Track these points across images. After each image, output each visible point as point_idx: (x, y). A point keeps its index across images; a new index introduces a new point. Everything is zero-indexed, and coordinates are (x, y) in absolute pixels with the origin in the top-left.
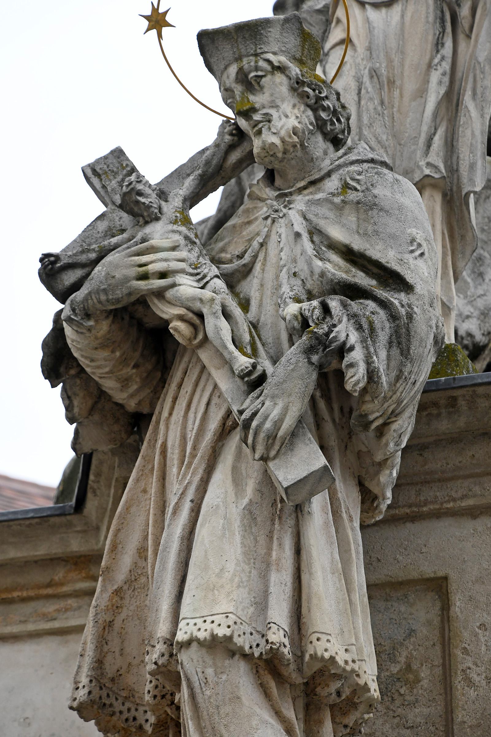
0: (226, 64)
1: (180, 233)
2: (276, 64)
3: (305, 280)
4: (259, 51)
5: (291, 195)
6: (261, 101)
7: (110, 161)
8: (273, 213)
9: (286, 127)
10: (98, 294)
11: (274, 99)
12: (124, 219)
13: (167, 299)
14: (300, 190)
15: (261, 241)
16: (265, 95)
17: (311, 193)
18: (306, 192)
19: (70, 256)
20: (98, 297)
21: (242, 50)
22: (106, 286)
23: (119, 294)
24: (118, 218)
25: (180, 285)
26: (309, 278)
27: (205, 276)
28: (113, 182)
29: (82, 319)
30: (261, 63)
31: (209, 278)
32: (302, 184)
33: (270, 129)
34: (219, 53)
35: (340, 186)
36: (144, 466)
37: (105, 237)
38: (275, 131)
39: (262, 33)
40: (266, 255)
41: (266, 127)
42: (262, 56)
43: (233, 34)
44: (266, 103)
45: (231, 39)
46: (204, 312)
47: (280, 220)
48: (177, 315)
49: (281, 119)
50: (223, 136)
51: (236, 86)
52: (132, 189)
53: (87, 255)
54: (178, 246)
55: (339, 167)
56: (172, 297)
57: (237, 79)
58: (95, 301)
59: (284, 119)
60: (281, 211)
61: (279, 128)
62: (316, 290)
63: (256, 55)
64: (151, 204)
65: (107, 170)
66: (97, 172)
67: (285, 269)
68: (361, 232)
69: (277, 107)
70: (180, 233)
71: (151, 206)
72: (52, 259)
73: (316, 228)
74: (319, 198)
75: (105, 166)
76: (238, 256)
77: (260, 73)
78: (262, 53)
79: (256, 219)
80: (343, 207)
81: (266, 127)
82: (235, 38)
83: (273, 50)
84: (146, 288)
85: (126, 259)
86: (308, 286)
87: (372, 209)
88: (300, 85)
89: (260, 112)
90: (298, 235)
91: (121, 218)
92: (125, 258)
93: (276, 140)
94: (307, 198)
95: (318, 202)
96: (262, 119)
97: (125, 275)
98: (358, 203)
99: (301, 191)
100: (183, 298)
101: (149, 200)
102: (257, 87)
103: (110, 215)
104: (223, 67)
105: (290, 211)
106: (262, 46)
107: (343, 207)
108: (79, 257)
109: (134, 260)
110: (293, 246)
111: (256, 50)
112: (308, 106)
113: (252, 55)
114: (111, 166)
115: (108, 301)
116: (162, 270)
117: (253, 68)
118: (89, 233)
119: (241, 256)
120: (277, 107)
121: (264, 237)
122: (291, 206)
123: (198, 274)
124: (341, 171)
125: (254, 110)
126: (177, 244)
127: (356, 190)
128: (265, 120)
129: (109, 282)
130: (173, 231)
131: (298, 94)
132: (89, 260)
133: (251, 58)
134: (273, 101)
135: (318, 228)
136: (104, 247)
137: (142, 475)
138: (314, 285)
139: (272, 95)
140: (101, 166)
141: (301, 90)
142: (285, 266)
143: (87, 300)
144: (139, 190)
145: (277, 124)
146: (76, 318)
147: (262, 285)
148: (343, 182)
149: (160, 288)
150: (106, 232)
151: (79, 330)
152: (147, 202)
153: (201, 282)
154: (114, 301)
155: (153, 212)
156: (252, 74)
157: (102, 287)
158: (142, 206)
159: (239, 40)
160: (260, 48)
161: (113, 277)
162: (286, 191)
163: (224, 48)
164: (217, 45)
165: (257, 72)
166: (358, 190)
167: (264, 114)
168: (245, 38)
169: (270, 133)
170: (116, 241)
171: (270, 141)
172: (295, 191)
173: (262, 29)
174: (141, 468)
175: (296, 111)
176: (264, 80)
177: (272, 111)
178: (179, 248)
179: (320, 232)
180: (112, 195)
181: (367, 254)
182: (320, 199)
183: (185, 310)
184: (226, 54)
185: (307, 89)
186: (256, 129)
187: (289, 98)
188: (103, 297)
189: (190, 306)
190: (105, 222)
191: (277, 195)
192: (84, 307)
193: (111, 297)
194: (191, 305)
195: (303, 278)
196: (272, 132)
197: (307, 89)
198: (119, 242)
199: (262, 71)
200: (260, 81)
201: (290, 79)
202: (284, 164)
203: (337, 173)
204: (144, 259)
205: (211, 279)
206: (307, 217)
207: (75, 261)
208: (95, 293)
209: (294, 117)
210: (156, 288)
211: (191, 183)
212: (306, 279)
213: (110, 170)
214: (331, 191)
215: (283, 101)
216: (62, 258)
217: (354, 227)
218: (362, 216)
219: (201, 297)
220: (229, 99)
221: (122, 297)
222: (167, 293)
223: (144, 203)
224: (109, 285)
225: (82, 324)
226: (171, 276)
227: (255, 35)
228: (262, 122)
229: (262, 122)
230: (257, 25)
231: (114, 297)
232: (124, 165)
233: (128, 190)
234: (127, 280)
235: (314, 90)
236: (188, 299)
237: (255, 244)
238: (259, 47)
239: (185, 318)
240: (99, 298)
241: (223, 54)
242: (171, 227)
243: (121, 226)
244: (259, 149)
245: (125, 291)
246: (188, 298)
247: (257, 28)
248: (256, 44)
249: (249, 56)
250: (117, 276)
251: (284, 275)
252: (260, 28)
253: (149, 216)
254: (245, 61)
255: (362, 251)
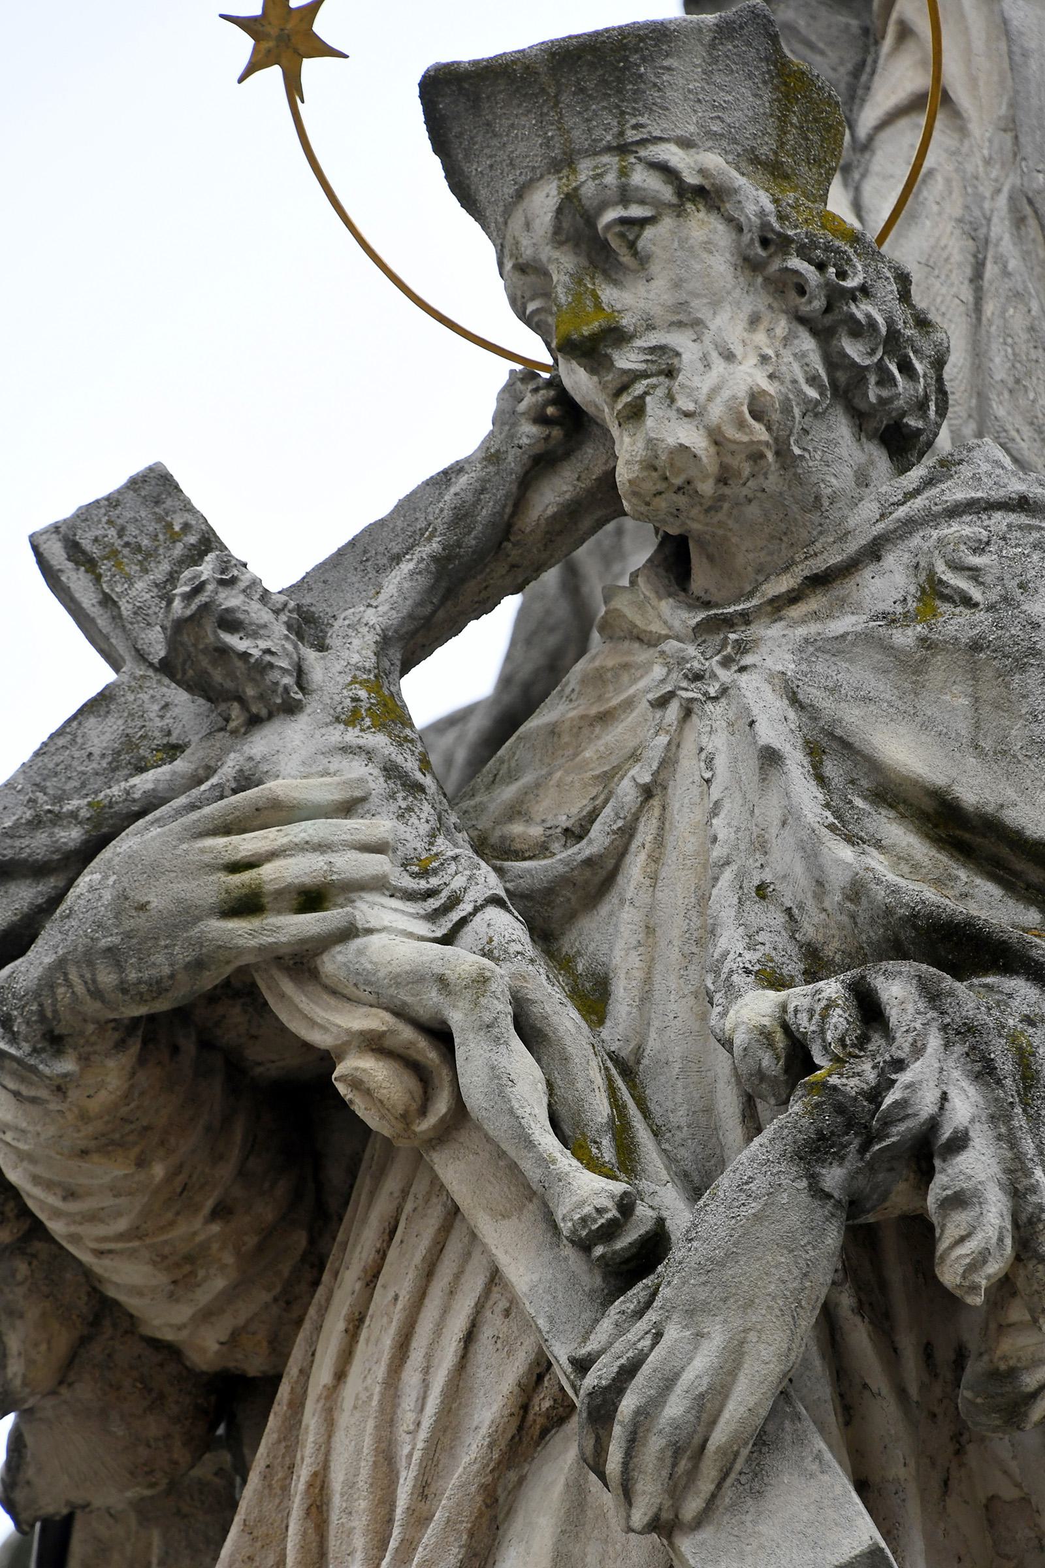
1: (368, 754)
2: (692, 179)
3: (795, 911)
4: (632, 136)
6: (642, 304)
9: (726, 394)
10: (91, 964)
11: (684, 297)
12: (176, 711)
13: (327, 981)
14: (778, 606)
15: (647, 778)
16: (654, 284)
17: (815, 616)
18: (796, 611)
20: (88, 976)
21: (576, 133)
22: (116, 940)
23: (160, 964)
24: (156, 707)
25: (369, 931)
26: (810, 903)
27: (454, 901)
29: (35, 1051)
30: (641, 178)
32: (783, 584)
33: (671, 398)
34: (495, 142)
35: (912, 589)
37: (114, 770)
38: (691, 407)
39: (641, 76)
40: (661, 828)
41: (660, 392)
42: (643, 153)
43: (544, 79)
44: (657, 311)
45: (536, 96)
46: (451, 1023)
47: (709, 707)
48: (362, 1033)
49: (708, 366)
50: (514, 425)
51: (556, 254)
52: (205, 607)
53: (51, 835)
54: (363, 799)
55: (910, 525)
56: (342, 974)
57: (557, 230)
58: (80, 989)
59: (719, 366)
60: (714, 676)
61: (702, 398)
62: (835, 944)
63: (623, 149)
64: (268, 658)
65: (118, 543)
66: (84, 552)
67: (728, 875)
68: (987, 744)
69: (696, 325)
70: (368, 754)
71: (271, 666)
73: (831, 735)
74: (841, 631)
75: (112, 532)
76: (567, 831)
77: (636, 211)
78: (643, 142)
79: (629, 704)
80: (924, 660)
81: (660, 392)
82: (552, 91)
83: (679, 132)
84: (253, 943)
85: (185, 846)
86: (809, 930)
87: (1023, 668)
88: (772, 249)
89: (638, 343)
90: (770, 758)
91: (166, 706)
92: (181, 840)
93: (691, 437)
94: (802, 631)
95: (838, 647)
96: (642, 366)
97: (180, 901)
98: (976, 646)
99: (779, 609)
100: (381, 974)
101: (263, 644)
102: (626, 258)
103: (131, 697)
104: (509, 190)
105: (744, 678)
107: (924, 660)
108: (26, 842)
109: (211, 850)
110: (753, 797)
111: (622, 134)
112: (802, 320)
113: (609, 149)
114: (132, 530)
115: (123, 988)
116: (307, 880)
117: (613, 193)
118: (57, 759)
119: (577, 830)
120: (696, 325)
121: (655, 767)
122: (748, 660)
124: (916, 541)
126: (358, 793)
127: (968, 602)
128: (654, 368)
129: (128, 924)
130: (346, 750)
131: (767, 280)
132: (57, 850)
133: (606, 159)
134: (682, 305)
135: (839, 732)
136: (111, 805)
138: (826, 926)
139: (677, 284)
141: (775, 265)
142: (728, 863)
143: (52, 987)
144: (227, 610)
145: (696, 382)
146: (13, 1051)
147: (650, 930)
148: (923, 577)
149: (303, 941)
151: (25, 1091)
152: (256, 653)
153: (442, 921)
154: (143, 988)
155: (277, 684)
156: (611, 215)
158: (239, 663)
159: (565, 98)
160: (635, 127)
161: (142, 907)
162: (731, 610)
163: (512, 126)
164: (490, 117)
165: (626, 207)
166: (976, 605)
167: (652, 350)
168: (582, 90)
169: (673, 414)
170: (150, 786)
171: (671, 441)
172: (759, 608)
173: (644, 59)
175: (760, 338)
176: (649, 232)
177: (680, 340)
178: (367, 807)
179: (846, 747)
181: (1008, 821)
182: (844, 636)
184: (522, 148)
185: (795, 263)
186: (625, 399)
187: (737, 293)
188: (107, 978)
189: (405, 1003)
190: (110, 720)
191: (698, 624)
192: (41, 1013)
193: (133, 976)
194: (409, 999)
195: (789, 904)
197: (795, 263)
198: (161, 786)
199: (642, 202)
200: (638, 237)
201: (740, 229)
202: (721, 516)
203: (902, 545)
204: (248, 844)
205: (477, 910)
206: (801, 697)
208: (77, 963)
209: (753, 360)
210: (289, 943)
211: (406, 585)
212: (801, 907)
213: (127, 544)
214: (881, 607)
215: (715, 304)
217: (963, 727)
218: (990, 692)
219: (441, 971)
220: (532, 299)
221: (172, 976)
222: (326, 957)
223: (245, 656)
224: (128, 935)
225: (33, 1069)
226: (340, 900)
227: (619, 80)
228: (645, 375)
229: (645, 375)
230: (624, 47)
231: (146, 975)
232: (177, 528)
233: (188, 613)
234: (188, 915)
235: (821, 267)
236: (397, 980)
237: (626, 791)
238: (634, 121)
239: (388, 1043)
240: (94, 981)
241: (510, 148)
243: (169, 734)
244: (637, 467)
245: (183, 955)
246: (399, 975)
247: (625, 59)
248: (623, 113)
249: (596, 154)
250: (155, 902)
251: (724, 892)
252: (635, 58)
253: (261, 697)
254: (585, 168)
255: (990, 809)
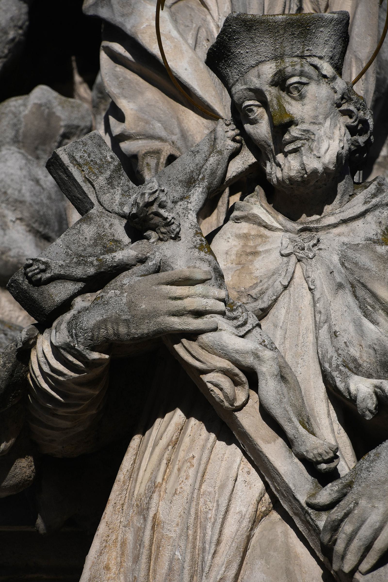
0: (260, 60)
3: (348, 344)
4: (307, 53)
5: (317, 232)
7: (90, 149)
8: (298, 251)
10: (117, 324)
19: (61, 266)
21: (287, 48)
22: (129, 317)
27: (245, 323)
28: (100, 178)
30: (308, 69)
31: (251, 327)
33: (311, 149)
34: (252, 44)
35: (379, 231)
36: (108, 536)
41: (306, 146)
44: (306, 117)
66: (76, 161)
72: (42, 267)
75: (86, 155)
77: (304, 80)
89: (298, 127)
91: (111, 225)
96: (300, 136)
97: (154, 308)
106: (311, 48)
111: (303, 52)
113: (297, 56)
114: (92, 155)
117: (297, 72)
123: (235, 318)
124: (377, 212)
125: (292, 122)
128: (304, 137)
130: (201, 259)
133: (296, 59)
137: (105, 546)
140: (82, 154)
150: (96, 240)
152: (170, 218)
153: (241, 329)
157: (123, 317)
167: (304, 131)
169: (313, 156)
174: (104, 538)
176: (305, 88)
180: (100, 194)
182: (358, 244)
183: (231, 364)
190: (92, 227)
192: (93, 337)
193: (133, 331)
194: (240, 359)
196: (314, 155)
199: (307, 77)
205: (254, 328)
207: (68, 272)
208: (112, 323)
211: (200, 196)
213: (92, 161)
216: (53, 265)
236: (237, 352)
238: (307, 48)
240: (117, 330)
242: (196, 253)
243: (114, 236)
